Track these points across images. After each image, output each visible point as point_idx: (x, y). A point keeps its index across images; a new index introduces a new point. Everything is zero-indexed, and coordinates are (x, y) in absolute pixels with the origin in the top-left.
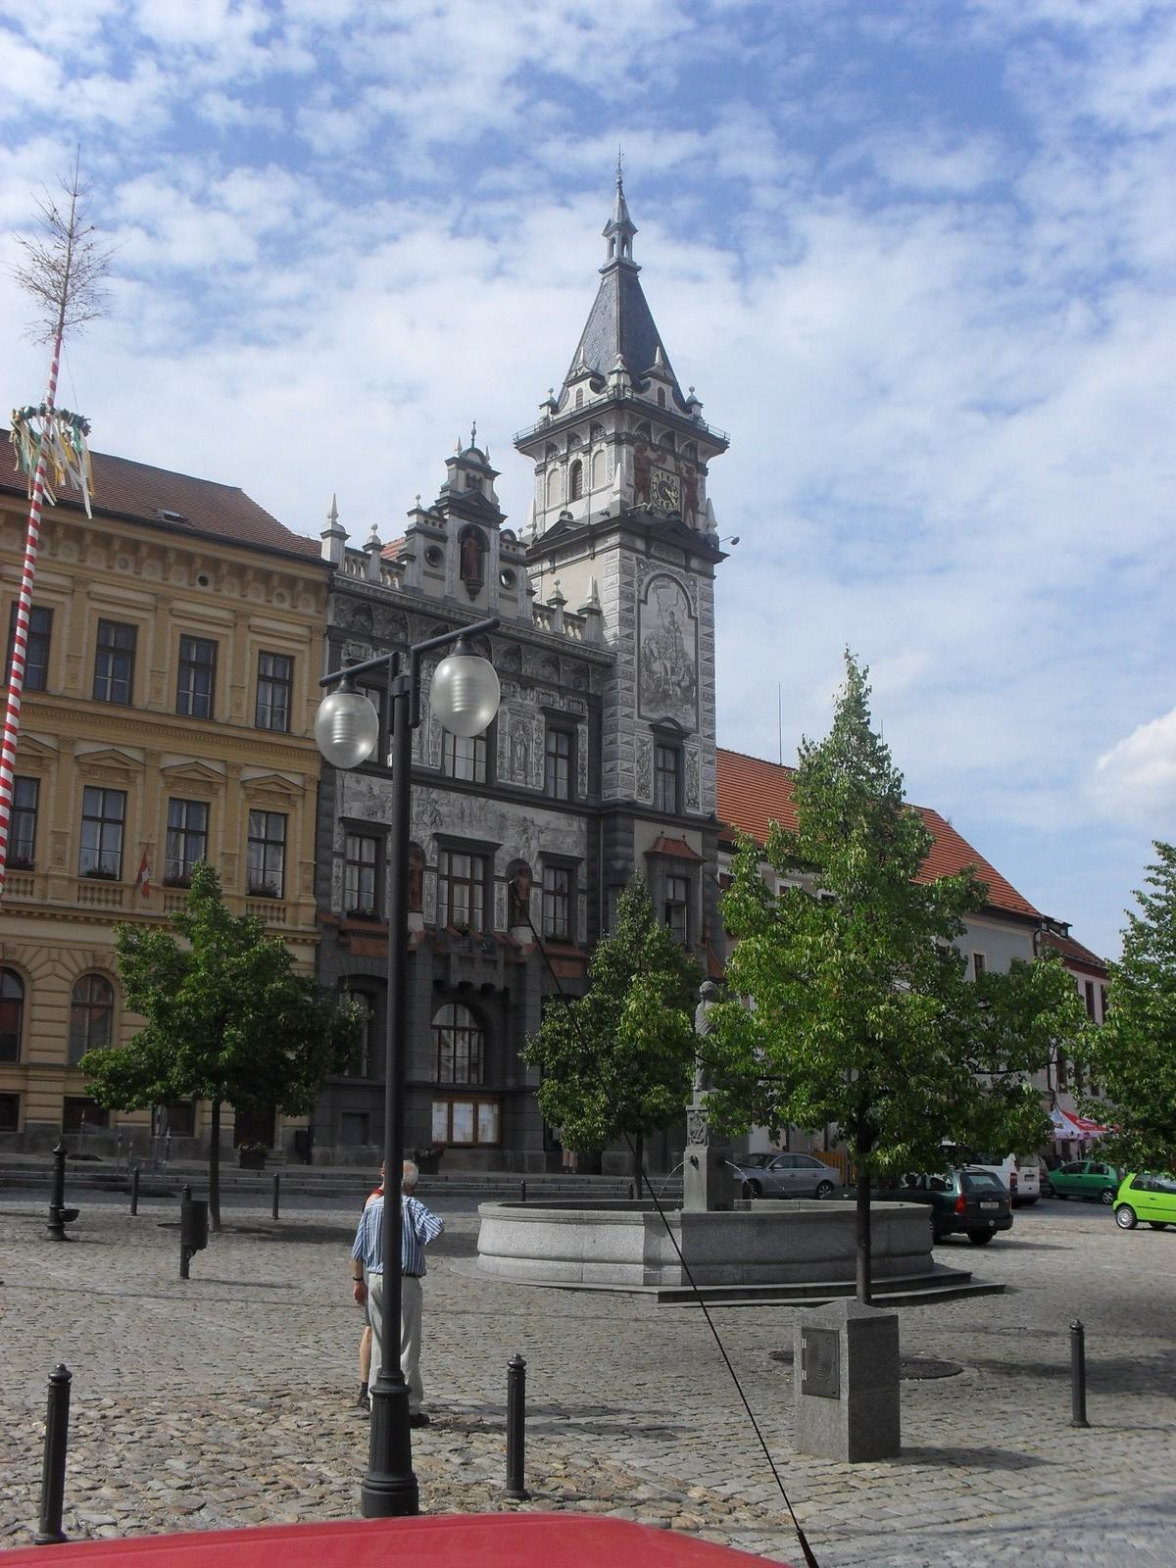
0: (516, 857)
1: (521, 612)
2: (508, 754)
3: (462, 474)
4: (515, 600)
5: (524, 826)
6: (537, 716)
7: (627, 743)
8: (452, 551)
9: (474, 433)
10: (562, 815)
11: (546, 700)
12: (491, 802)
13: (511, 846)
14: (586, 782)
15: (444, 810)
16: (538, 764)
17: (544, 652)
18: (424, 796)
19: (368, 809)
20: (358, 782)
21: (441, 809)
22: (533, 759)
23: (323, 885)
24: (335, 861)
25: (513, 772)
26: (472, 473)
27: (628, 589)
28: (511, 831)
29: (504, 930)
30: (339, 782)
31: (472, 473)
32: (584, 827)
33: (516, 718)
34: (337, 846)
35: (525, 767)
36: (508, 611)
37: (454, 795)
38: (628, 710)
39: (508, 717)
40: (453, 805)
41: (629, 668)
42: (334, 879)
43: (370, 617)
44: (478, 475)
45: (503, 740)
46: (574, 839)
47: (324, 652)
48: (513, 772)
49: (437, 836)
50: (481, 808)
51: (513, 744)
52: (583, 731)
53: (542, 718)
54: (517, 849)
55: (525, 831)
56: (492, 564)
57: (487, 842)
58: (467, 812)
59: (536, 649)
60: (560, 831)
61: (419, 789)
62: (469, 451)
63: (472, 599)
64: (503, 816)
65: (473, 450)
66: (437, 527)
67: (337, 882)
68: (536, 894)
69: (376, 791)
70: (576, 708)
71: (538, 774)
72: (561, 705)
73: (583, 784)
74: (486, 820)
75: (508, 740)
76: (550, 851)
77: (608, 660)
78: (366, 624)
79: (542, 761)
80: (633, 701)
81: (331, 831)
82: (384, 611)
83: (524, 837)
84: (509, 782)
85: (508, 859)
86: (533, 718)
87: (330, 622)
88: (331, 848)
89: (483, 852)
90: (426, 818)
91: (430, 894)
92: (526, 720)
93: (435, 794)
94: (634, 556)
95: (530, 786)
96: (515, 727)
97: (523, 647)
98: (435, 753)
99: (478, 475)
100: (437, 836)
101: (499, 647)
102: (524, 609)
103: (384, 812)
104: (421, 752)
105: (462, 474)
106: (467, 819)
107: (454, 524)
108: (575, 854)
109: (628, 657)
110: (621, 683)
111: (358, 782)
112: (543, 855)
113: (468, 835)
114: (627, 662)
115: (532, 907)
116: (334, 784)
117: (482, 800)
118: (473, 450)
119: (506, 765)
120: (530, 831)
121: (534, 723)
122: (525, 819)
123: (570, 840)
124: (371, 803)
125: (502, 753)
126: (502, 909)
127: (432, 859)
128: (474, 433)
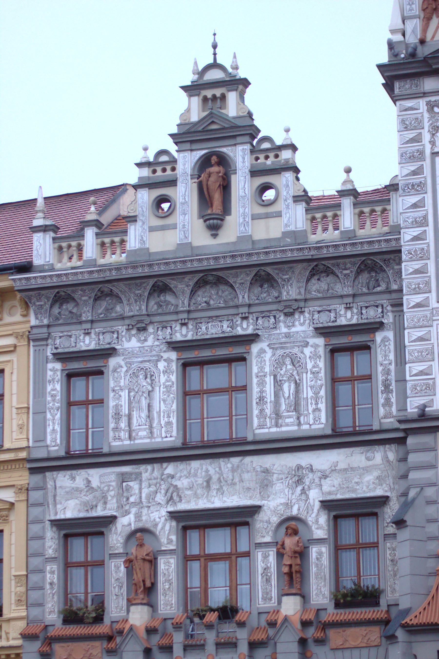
0: (288, 514)
1: (286, 225)
2: (270, 396)
3: (196, 101)
4: (279, 215)
5: (298, 477)
6: (312, 341)
7: (421, 339)
8: (185, 193)
9: (215, 46)
10: (357, 450)
11: (324, 320)
12: (248, 459)
13: (275, 504)
14: (393, 400)
15: (182, 483)
16: (316, 399)
17: (300, 266)
18: (156, 474)
19: (85, 504)
20: (73, 478)
21: (179, 484)
22: (307, 393)
23: (34, 595)
24: (48, 568)
25: (278, 415)
26: (209, 93)
27: (415, 146)
28: (278, 486)
29: (274, 603)
30: (50, 484)
31: (209, 93)
32: (391, 456)
33: (280, 352)
34: (50, 551)
35: (296, 407)
36: (268, 231)
37: (195, 464)
38: (418, 298)
39: (269, 353)
40: (196, 475)
41: (419, 245)
42: (48, 586)
43: (77, 305)
44: (218, 92)
45: (262, 383)
46: (376, 473)
47: (29, 355)
48: (278, 415)
49: (174, 516)
50: (233, 470)
51: (278, 384)
52: (385, 340)
53: (321, 341)
54: (288, 505)
55: (299, 481)
56: (242, 185)
57: (238, 508)
58: (215, 478)
59: (286, 266)
60: (352, 469)
61: (149, 467)
62: (208, 67)
63: (215, 236)
64: (266, 471)
65: (215, 65)
66: (169, 172)
67: (52, 588)
68: (320, 554)
69: (95, 483)
70: (372, 314)
71: (317, 410)
72: (347, 318)
73: (388, 403)
74: (242, 481)
75: (269, 380)
76: (339, 497)
77: (394, 243)
78: (75, 311)
79: (323, 393)
80: (428, 283)
81: (42, 538)
82: (84, 291)
83: (299, 488)
84: (274, 430)
85: (275, 520)
86: (307, 344)
87: (33, 321)
88: (41, 555)
89: (239, 518)
90: (160, 498)
91: (170, 582)
92: (296, 350)
93: (170, 469)
94: (422, 104)
95: (305, 427)
96: (279, 363)
97: (269, 269)
98: (169, 424)
99: (218, 92)
100: (174, 516)
101: (239, 280)
102: (296, 218)
103: (105, 503)
104: (151, 427)
105: (196, 101)
106: (214, 486)
107: (187, 162)
108: (379, 492)
109: (416, 232)
110: (408, 267)
111: (73, 478)
112: (327, 505)
113: (218, 503)
114: (416, 238)
115: (313, 569)
116: (43, 488)
117: (235, 460)
118: (215, 65)
119: (268, 410)
120: (307, 481)
121: (308, 351)
122: (299, 467)
123: (369, 478)
124: (89, 498)
125: (261, 399)
126: (268, 581)
127: (170, 542)
128: (215, 46)
